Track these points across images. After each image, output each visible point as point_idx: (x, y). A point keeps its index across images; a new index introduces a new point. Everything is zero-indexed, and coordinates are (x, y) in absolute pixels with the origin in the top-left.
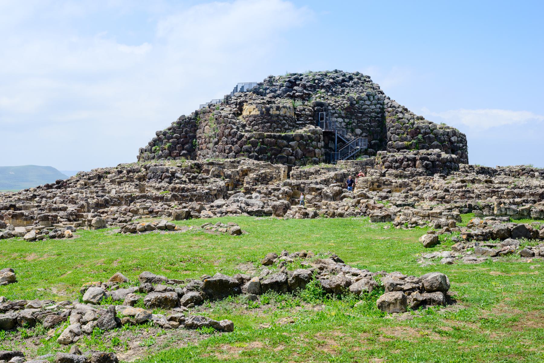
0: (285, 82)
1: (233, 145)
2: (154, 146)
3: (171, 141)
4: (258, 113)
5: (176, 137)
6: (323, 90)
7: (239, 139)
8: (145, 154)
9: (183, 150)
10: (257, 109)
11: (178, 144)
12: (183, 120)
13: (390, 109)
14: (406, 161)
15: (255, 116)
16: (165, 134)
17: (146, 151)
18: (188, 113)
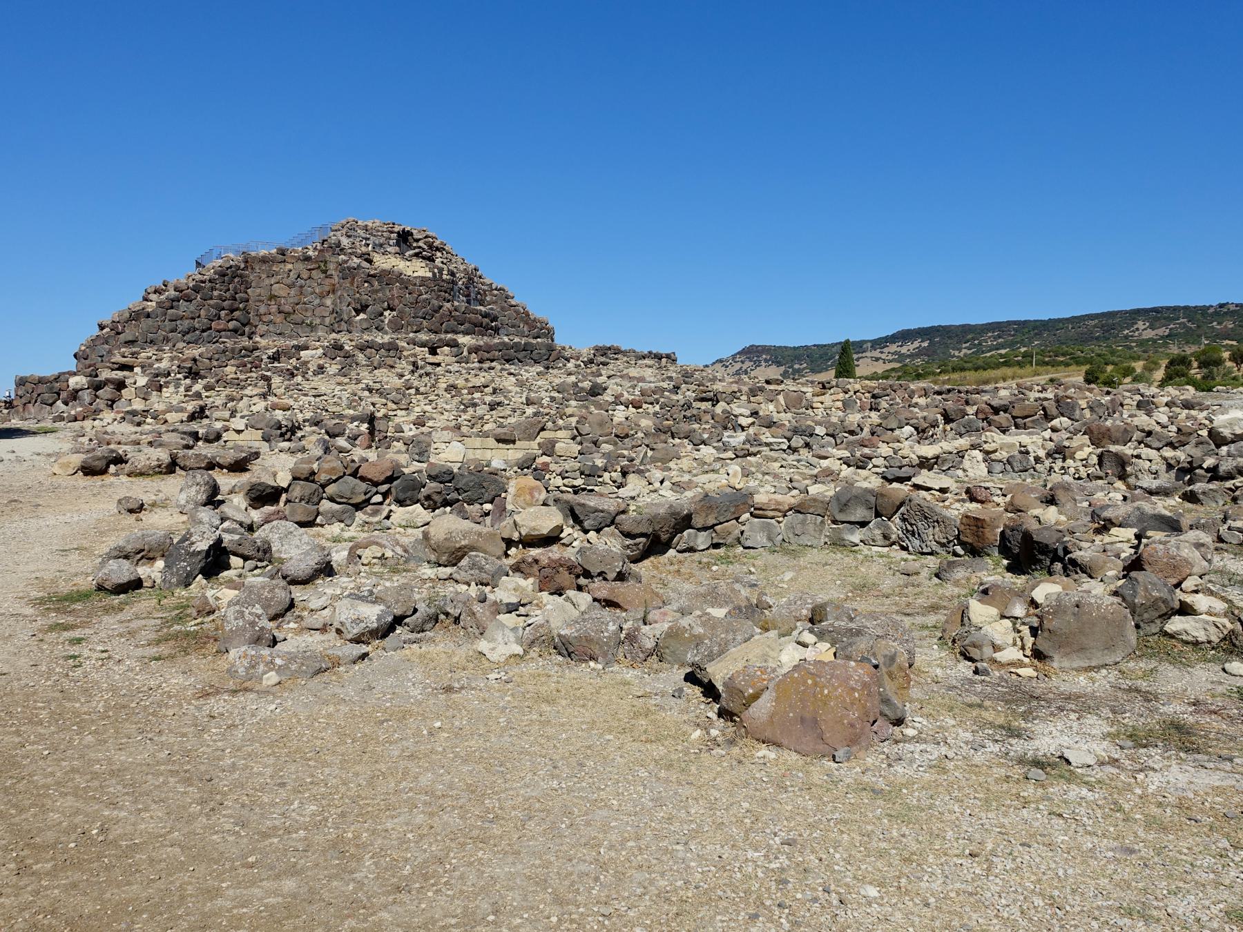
0: (392, 232)
1: (424, 318)
2: (172, 308)
3: (211, 302)
4: (430, 275)
5: (220, 298)
6: (439, 254)
7: (436, 312)
8: (145, 323)
9: (232, 320)
10: (427, 269)
11: (223, 309)
12: (227, 268)
13: (495, 292)
15: (423, 279)
16: (196, 289)
17: (148, 316)
18: (235, 258)
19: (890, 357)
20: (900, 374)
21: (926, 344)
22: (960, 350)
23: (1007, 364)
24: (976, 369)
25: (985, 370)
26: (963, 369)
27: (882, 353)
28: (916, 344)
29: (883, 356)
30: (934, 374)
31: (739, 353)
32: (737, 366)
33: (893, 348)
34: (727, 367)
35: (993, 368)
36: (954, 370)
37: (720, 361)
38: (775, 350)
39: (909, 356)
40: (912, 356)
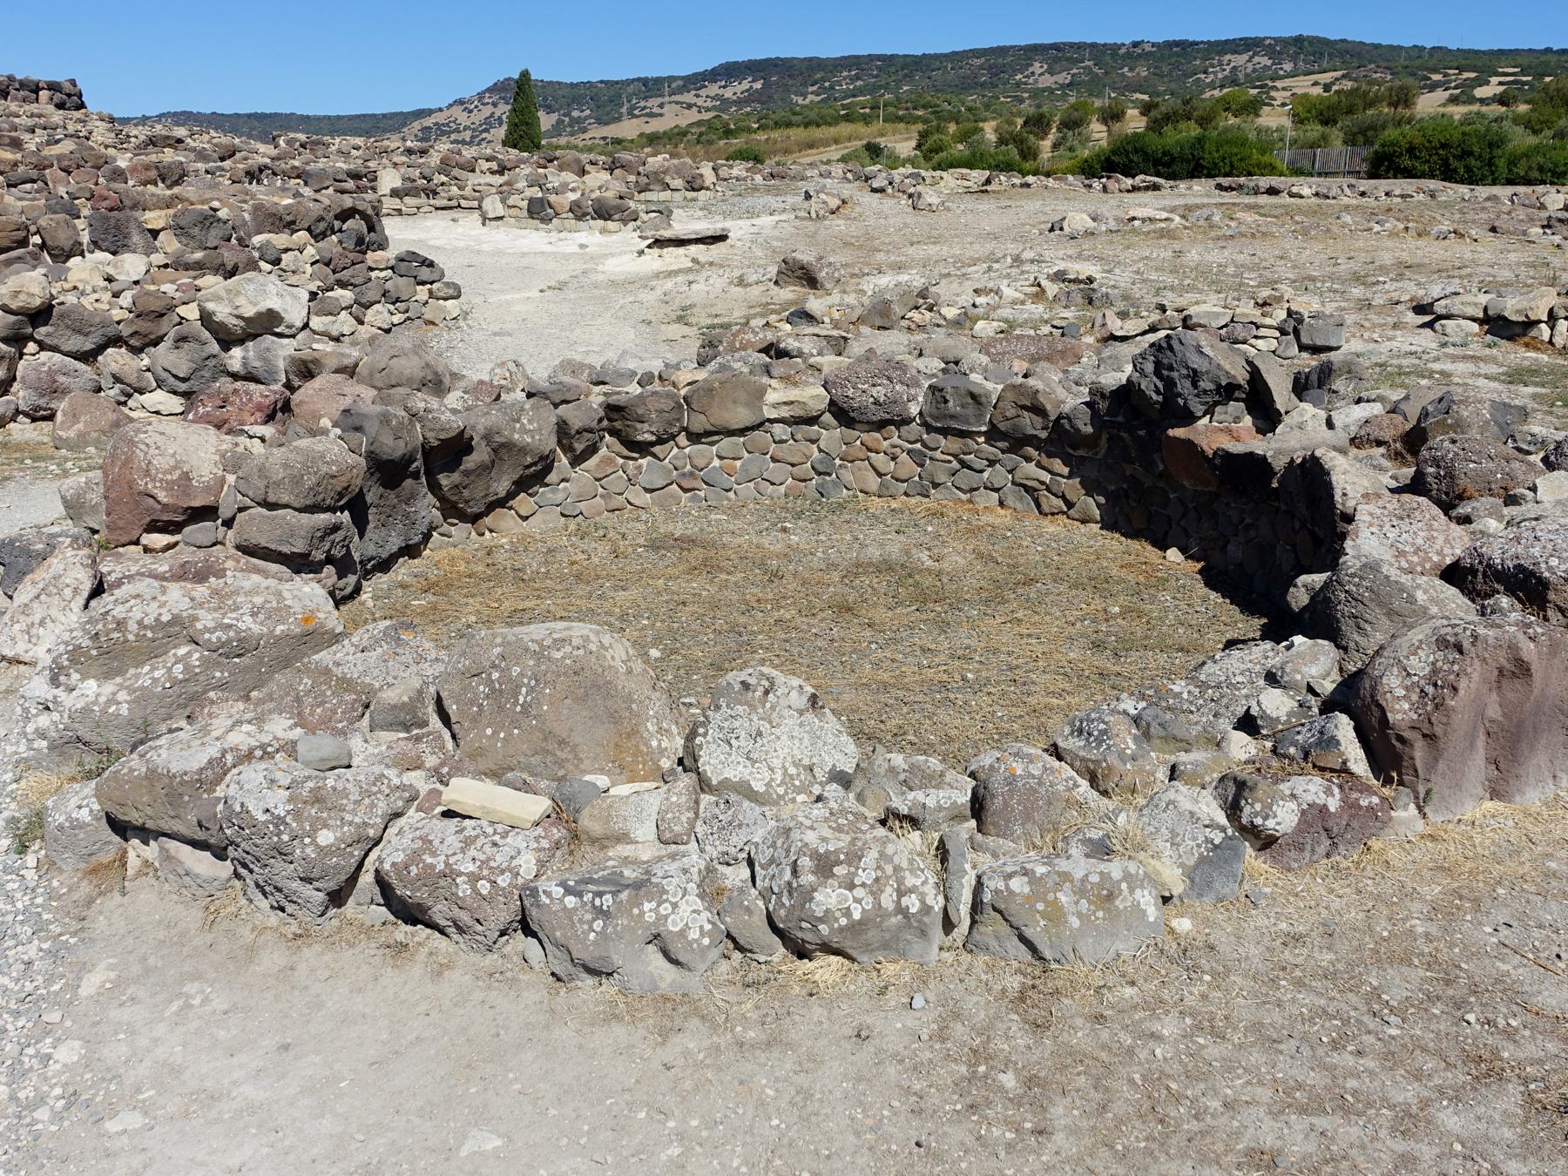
14: (17, 90)
19: (709, 104)
20: (703, 129)
21: (758, 85)
22: (804, 96)
23: (848, 118)
24: (806, 125)
25: (818, 126)
26: (789, 125)
27: (697, 96)
28: (745, 85)
29: (700, 102)
30: (749, 130)
31: (489, 90)
32: (487, 111)
33: (713, 89)
34: (471, 111)
35: (830, 124)
36: (777, 125)
37: (460, 102)
38: (543, 87)
39: (735, 103)
40: (739, 103)
